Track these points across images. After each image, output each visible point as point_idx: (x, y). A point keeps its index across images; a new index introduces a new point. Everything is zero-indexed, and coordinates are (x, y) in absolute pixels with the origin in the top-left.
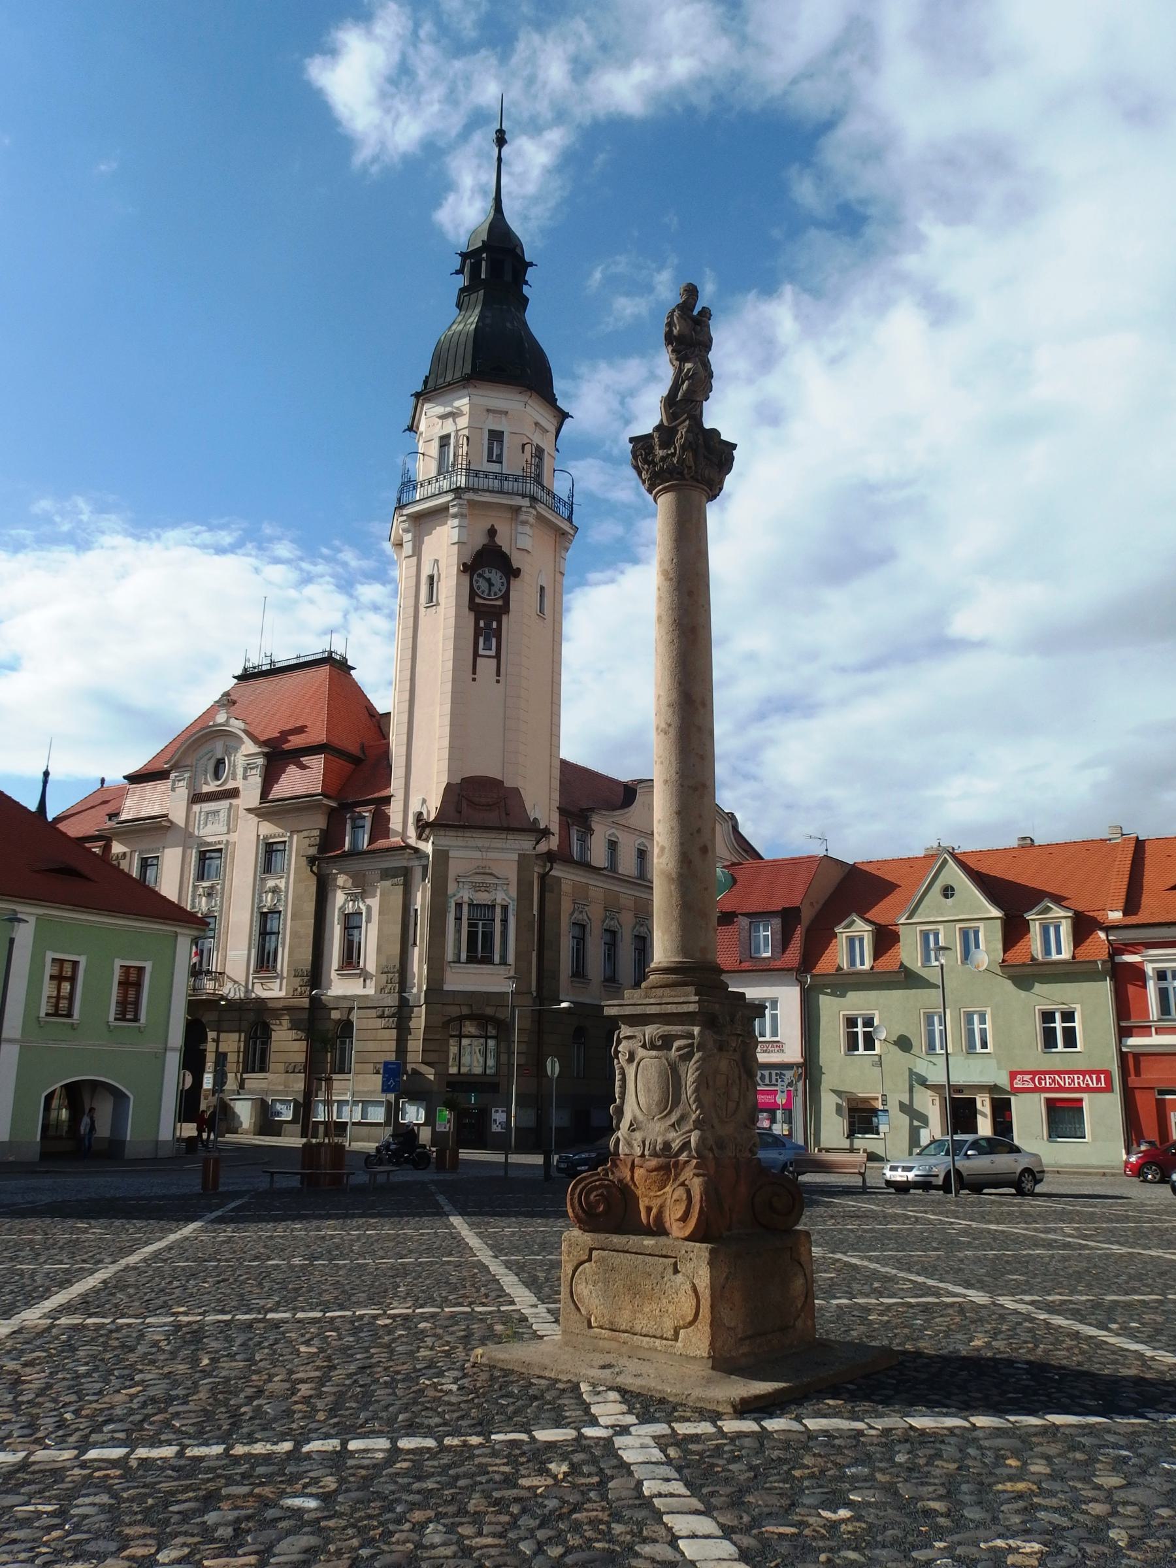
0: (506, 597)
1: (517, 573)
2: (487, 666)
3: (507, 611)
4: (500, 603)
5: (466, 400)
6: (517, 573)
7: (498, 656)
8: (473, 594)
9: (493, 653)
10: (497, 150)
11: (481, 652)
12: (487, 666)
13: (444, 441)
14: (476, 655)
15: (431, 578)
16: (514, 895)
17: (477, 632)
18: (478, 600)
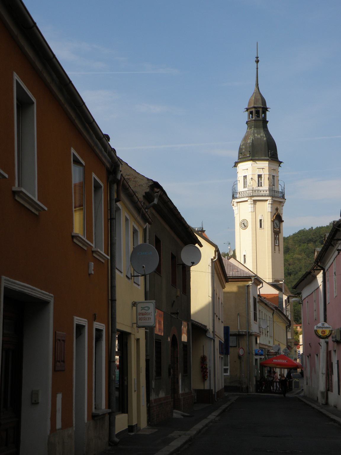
0: (280, 229)
1: (283, 221)
2: (277, 248)
3: (280, 233)
4: (278, 230)
5: (267, 165)
6: (283, 221)
7: (279, 246)
8: (274, 228)
9: (278, 245)
10: (256, 64)
11: (276, 244)
12: (277, 248)
13: (260, 176)
14: (275, 245)
15: (261, 220)
16: (290, 313)
17: (275, 239)
18: (275, 229)
